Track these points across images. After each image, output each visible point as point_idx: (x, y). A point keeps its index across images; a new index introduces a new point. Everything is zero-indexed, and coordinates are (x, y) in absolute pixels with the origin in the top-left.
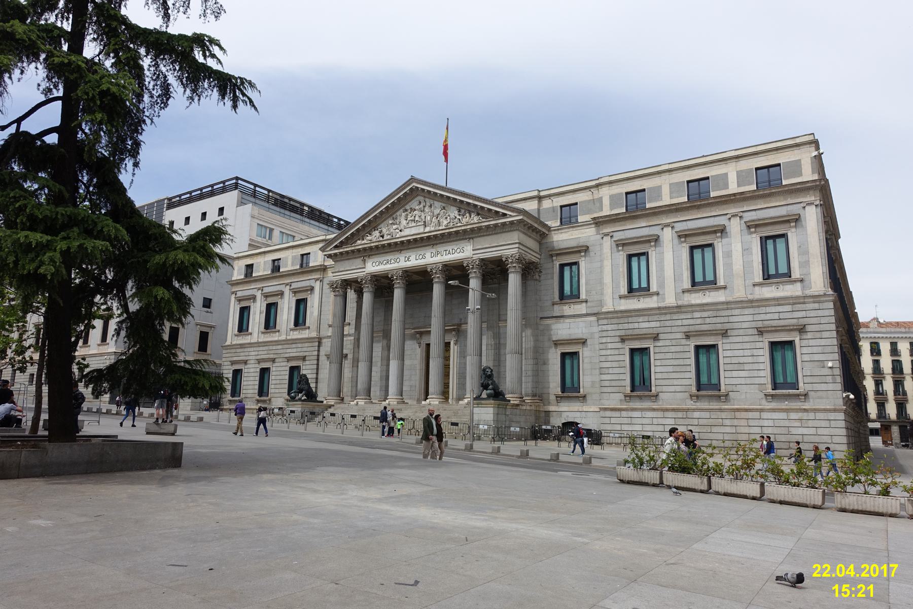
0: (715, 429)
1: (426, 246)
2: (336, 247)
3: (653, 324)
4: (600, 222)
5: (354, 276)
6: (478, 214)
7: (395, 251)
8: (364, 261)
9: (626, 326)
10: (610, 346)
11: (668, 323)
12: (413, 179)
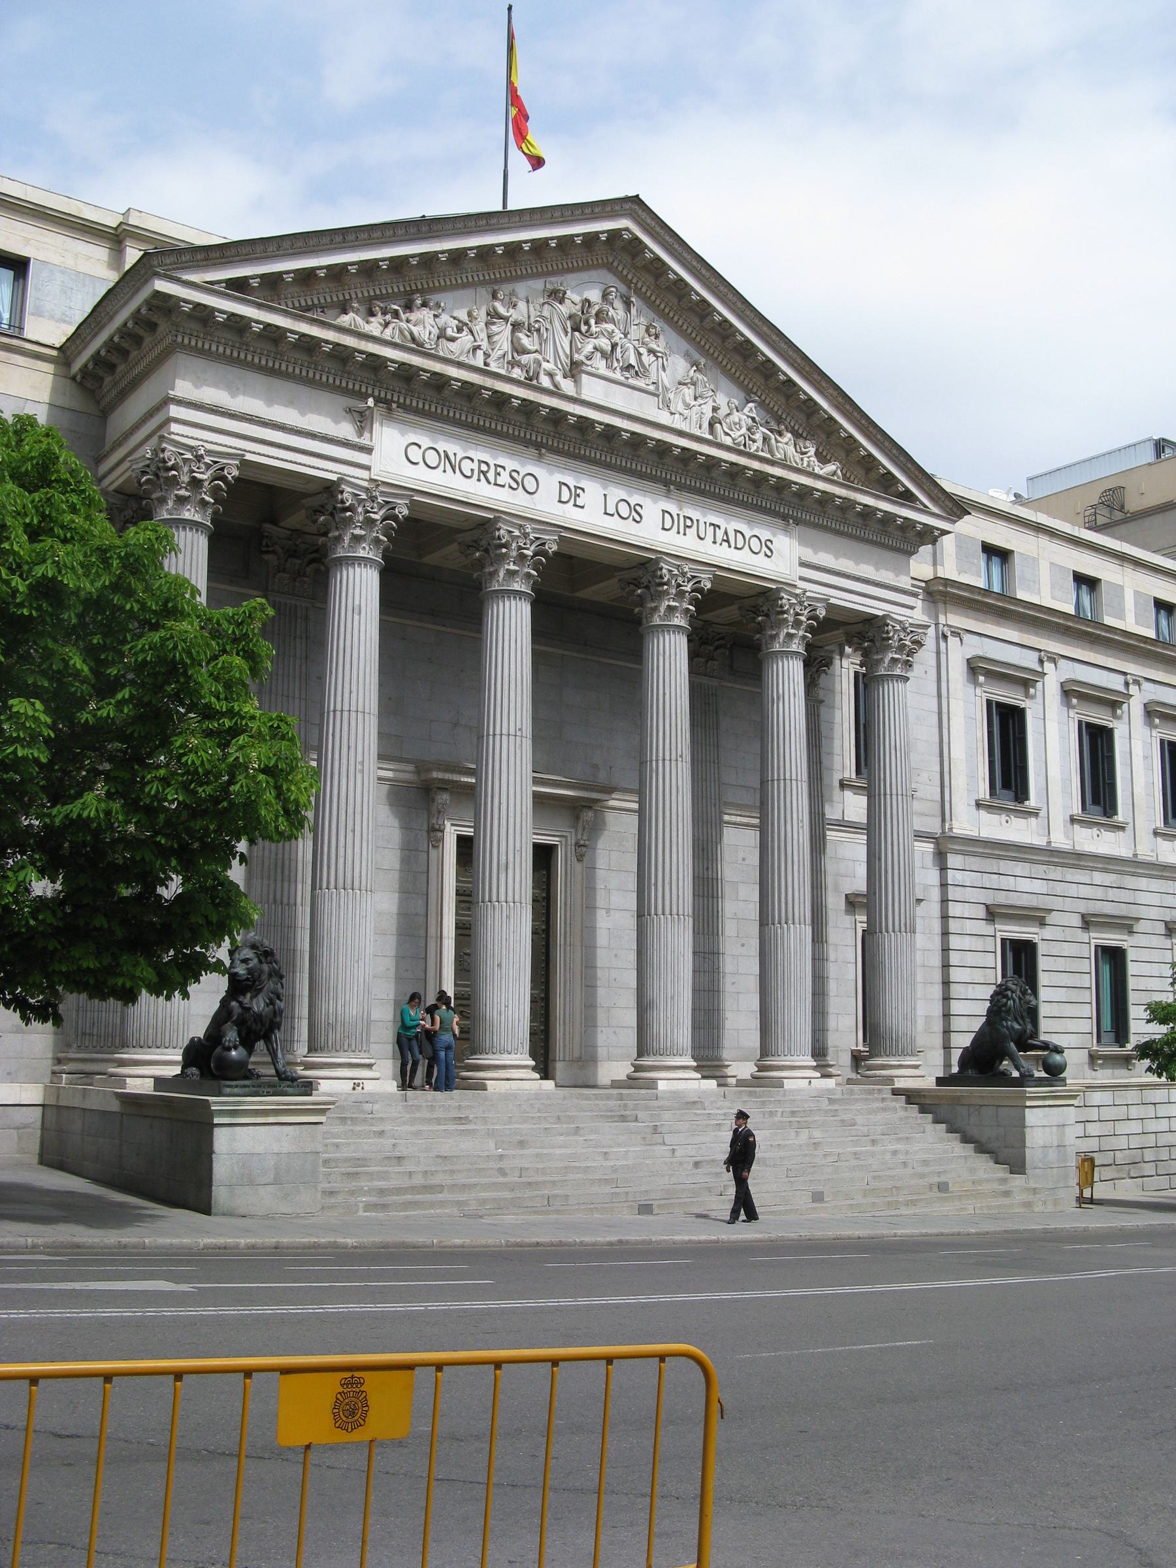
0: (1122, 1128)
1: (642, 476)
2: (238, 286)
3: (1038, 886)
4: (945, 594)
5: (328, 472)
6: (817, 454)
7: (515, 439)
8: (363, 421)
9: (994, 881)
10: (970, 926)
11: (1059, 888)
12: (634, 205)
